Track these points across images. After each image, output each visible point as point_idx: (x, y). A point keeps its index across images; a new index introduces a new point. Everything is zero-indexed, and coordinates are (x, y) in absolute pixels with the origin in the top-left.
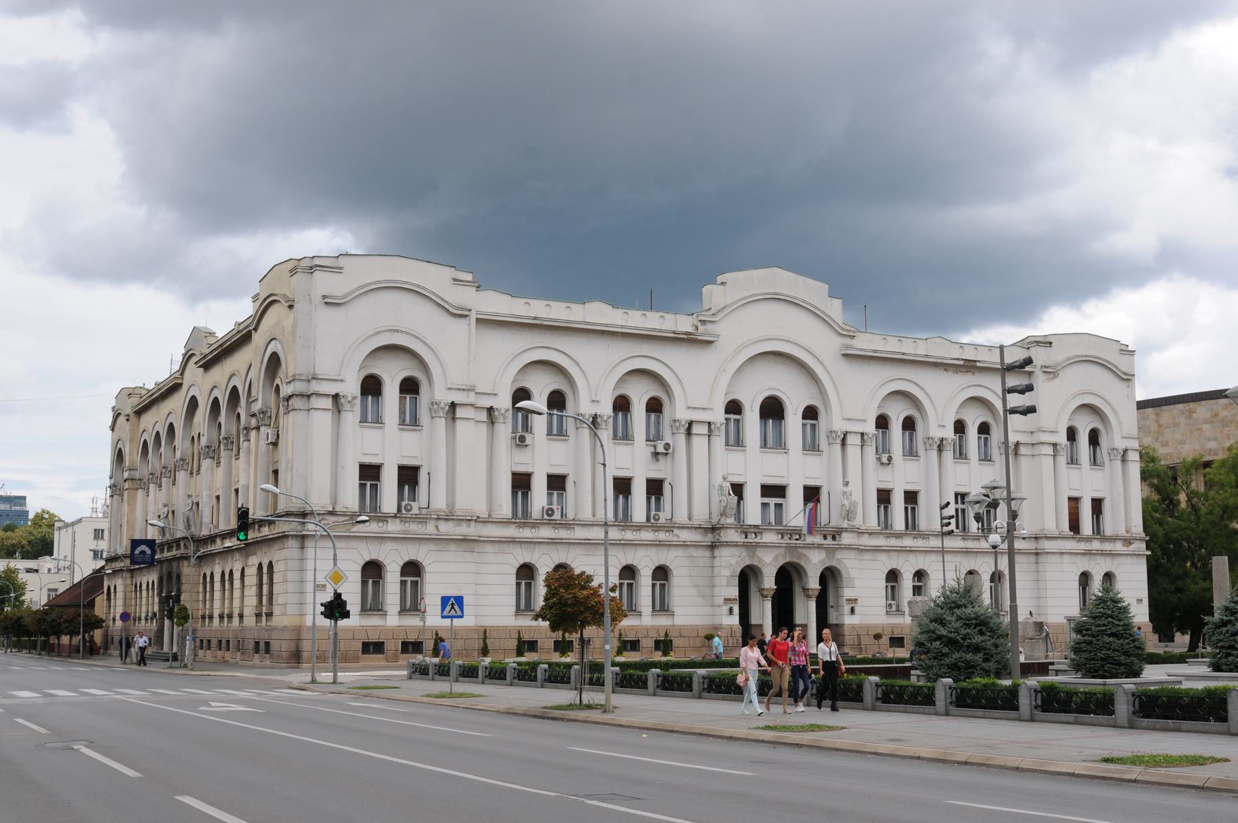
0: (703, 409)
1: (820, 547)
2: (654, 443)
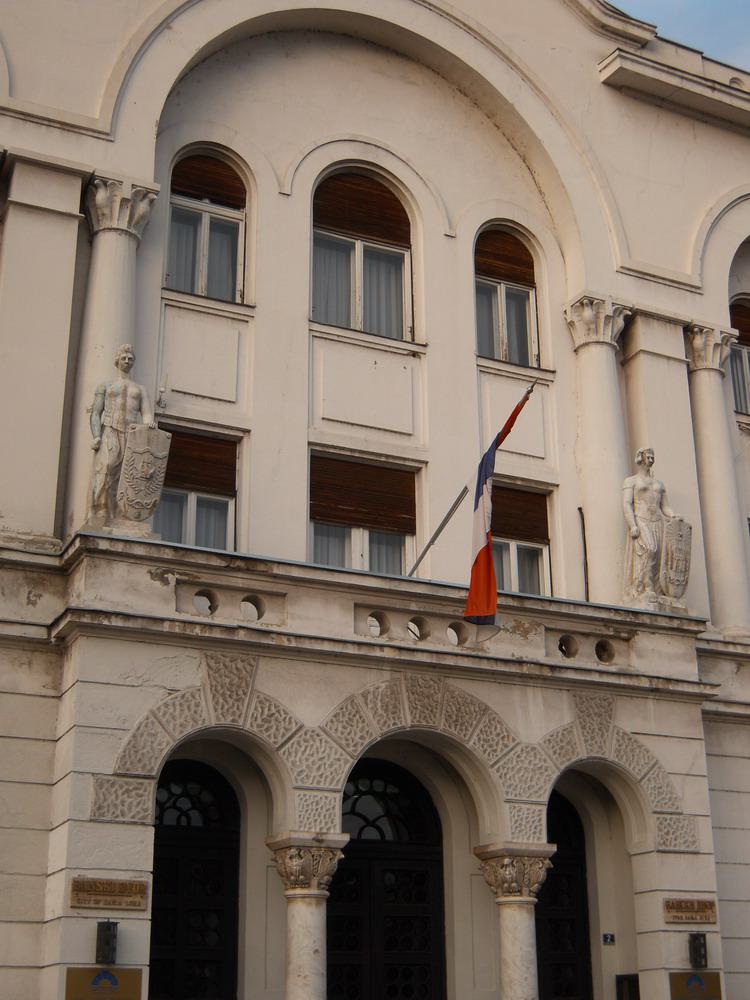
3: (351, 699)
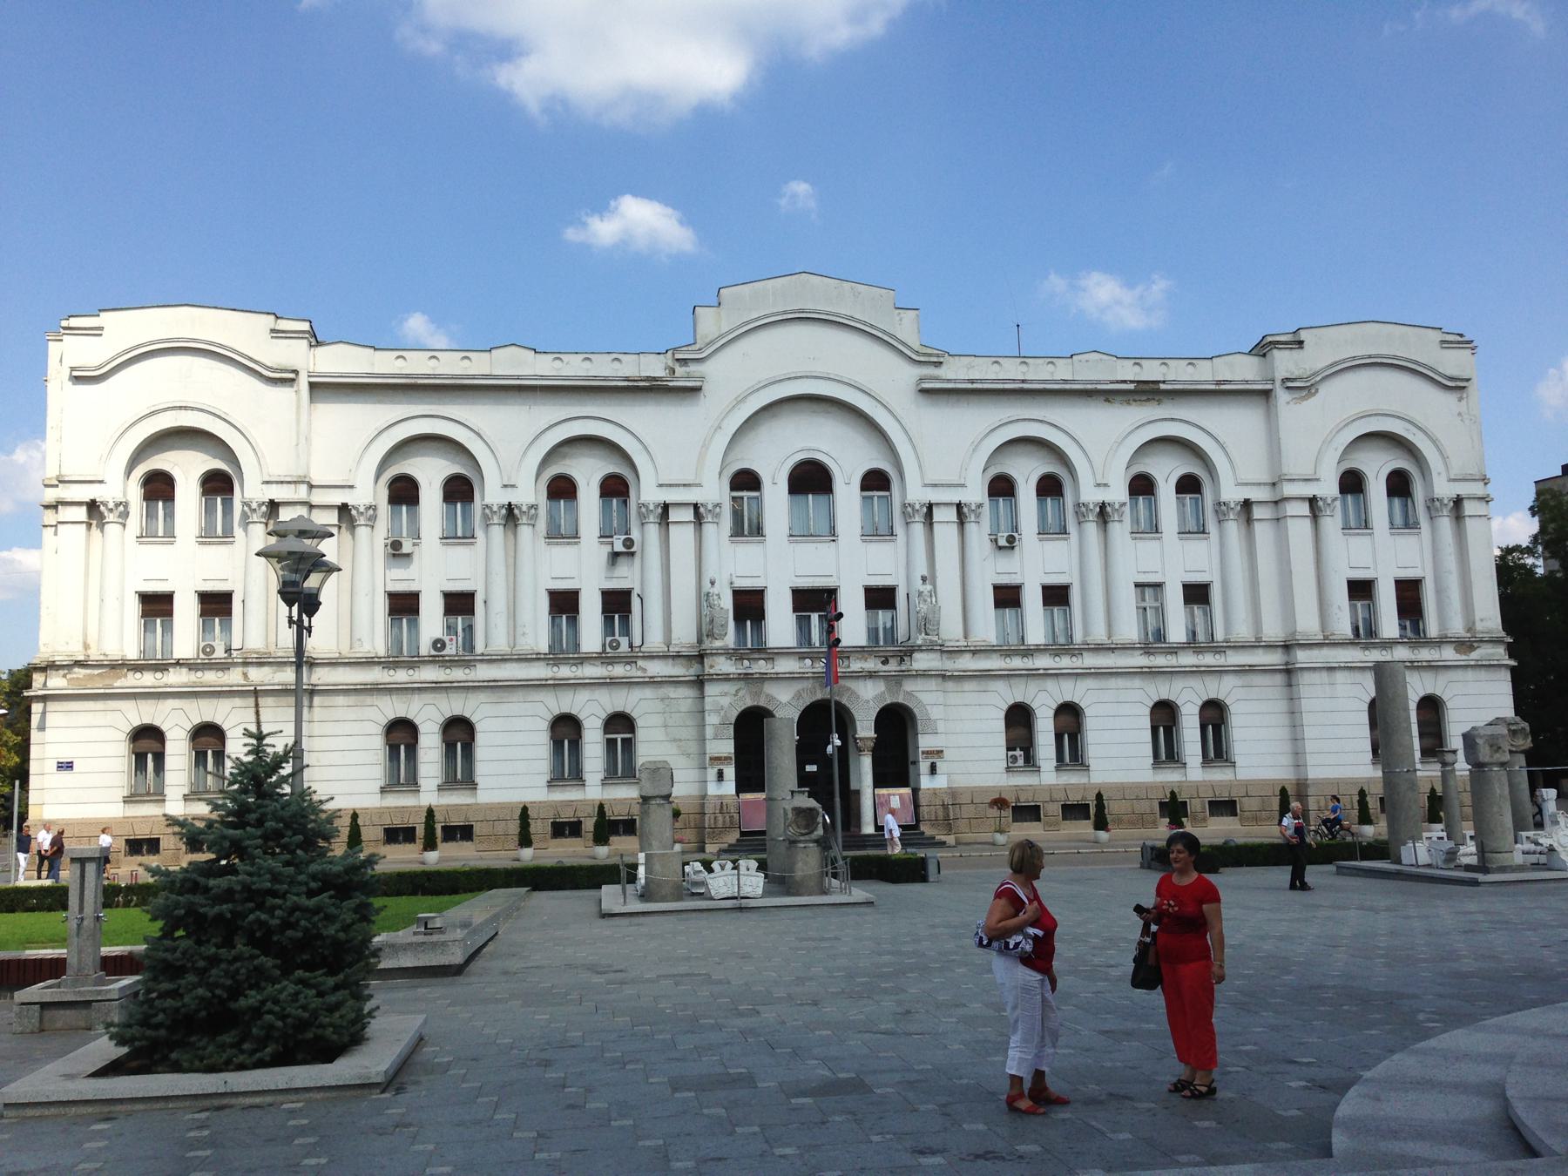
0: (684, 485)
1: (872, 675)
2: (610, 540)
3: (798, 691)
